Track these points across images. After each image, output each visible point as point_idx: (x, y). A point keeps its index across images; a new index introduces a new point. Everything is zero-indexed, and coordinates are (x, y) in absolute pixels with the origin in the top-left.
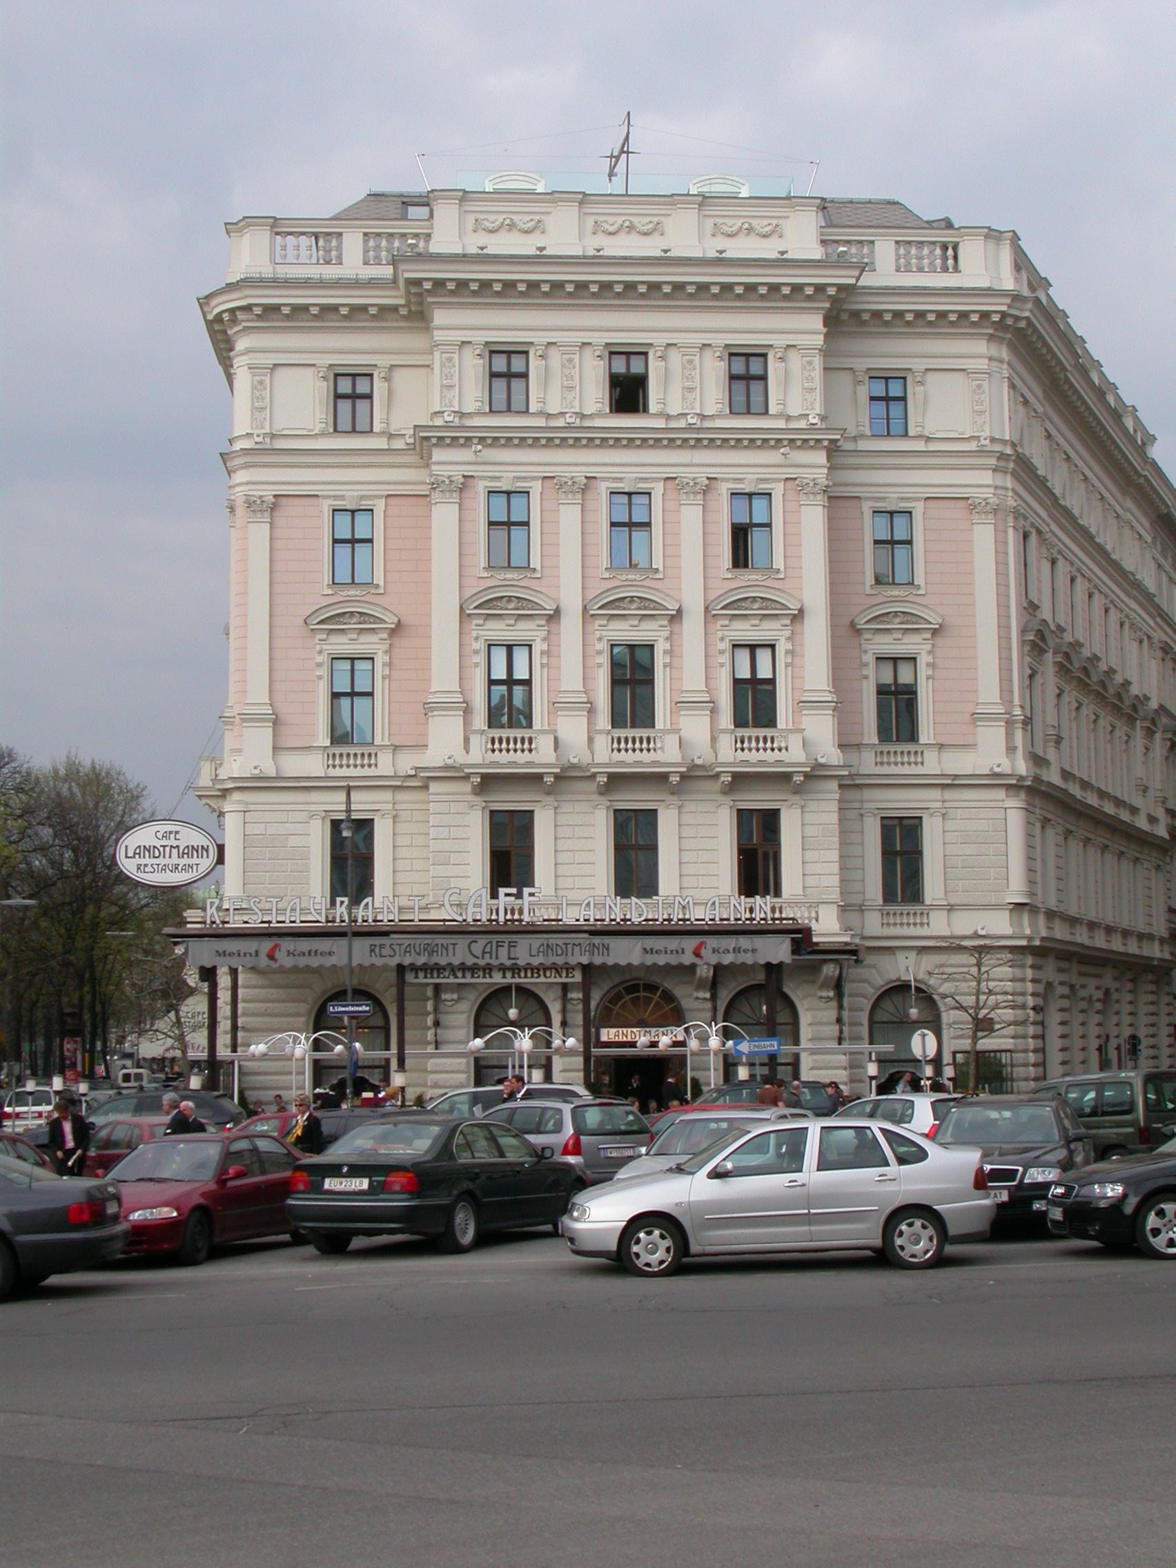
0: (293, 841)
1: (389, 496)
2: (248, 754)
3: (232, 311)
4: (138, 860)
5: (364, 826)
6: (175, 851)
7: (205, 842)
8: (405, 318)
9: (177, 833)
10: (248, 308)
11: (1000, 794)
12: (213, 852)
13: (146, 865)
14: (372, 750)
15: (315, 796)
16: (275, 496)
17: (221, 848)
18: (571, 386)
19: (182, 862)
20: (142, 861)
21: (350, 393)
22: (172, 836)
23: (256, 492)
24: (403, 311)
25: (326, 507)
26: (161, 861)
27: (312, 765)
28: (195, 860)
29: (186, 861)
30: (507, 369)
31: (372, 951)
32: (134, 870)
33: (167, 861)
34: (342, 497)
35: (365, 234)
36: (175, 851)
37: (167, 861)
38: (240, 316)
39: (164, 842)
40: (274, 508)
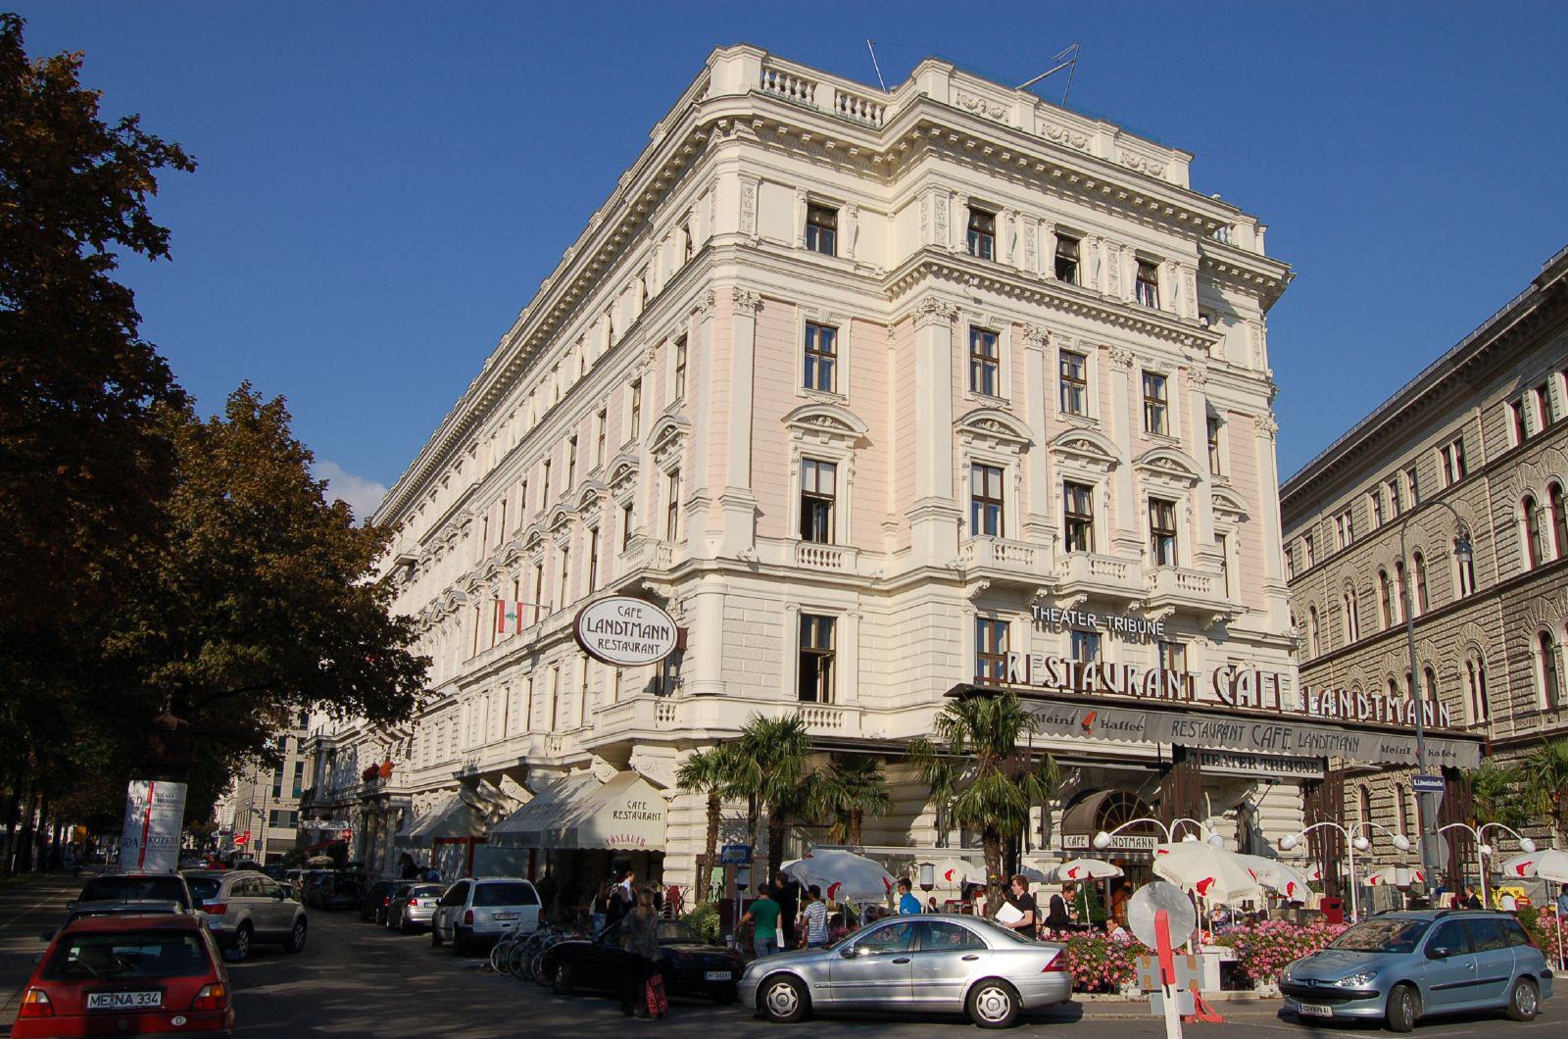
0: (766, 630)
1: (854, 319)
2: (715, 536)
3: (732, 120)
4: (599, 635)
5: (827, 623)
6: (636, 629)
7: (666, 625)
9: (639, 610)
10: (747, 120)
13: (607, 641)
14: (832, 550)
15: (786, 587)
16: (763, 297)
17: (682, 634)
19: (643, 641)
20: (604, 636)
21: (821, 222)
22: (635, 613)
23: (745, 287)
24: (877, 159)
26: (622, 638)
28: (655, 642)
29: (643, 641)
31: (1175, 728)
32: (596, 645)
35: (837, 91)
36: (636, 629)
38: (738, 125)
39: (627, 619)
40: (759, 307)
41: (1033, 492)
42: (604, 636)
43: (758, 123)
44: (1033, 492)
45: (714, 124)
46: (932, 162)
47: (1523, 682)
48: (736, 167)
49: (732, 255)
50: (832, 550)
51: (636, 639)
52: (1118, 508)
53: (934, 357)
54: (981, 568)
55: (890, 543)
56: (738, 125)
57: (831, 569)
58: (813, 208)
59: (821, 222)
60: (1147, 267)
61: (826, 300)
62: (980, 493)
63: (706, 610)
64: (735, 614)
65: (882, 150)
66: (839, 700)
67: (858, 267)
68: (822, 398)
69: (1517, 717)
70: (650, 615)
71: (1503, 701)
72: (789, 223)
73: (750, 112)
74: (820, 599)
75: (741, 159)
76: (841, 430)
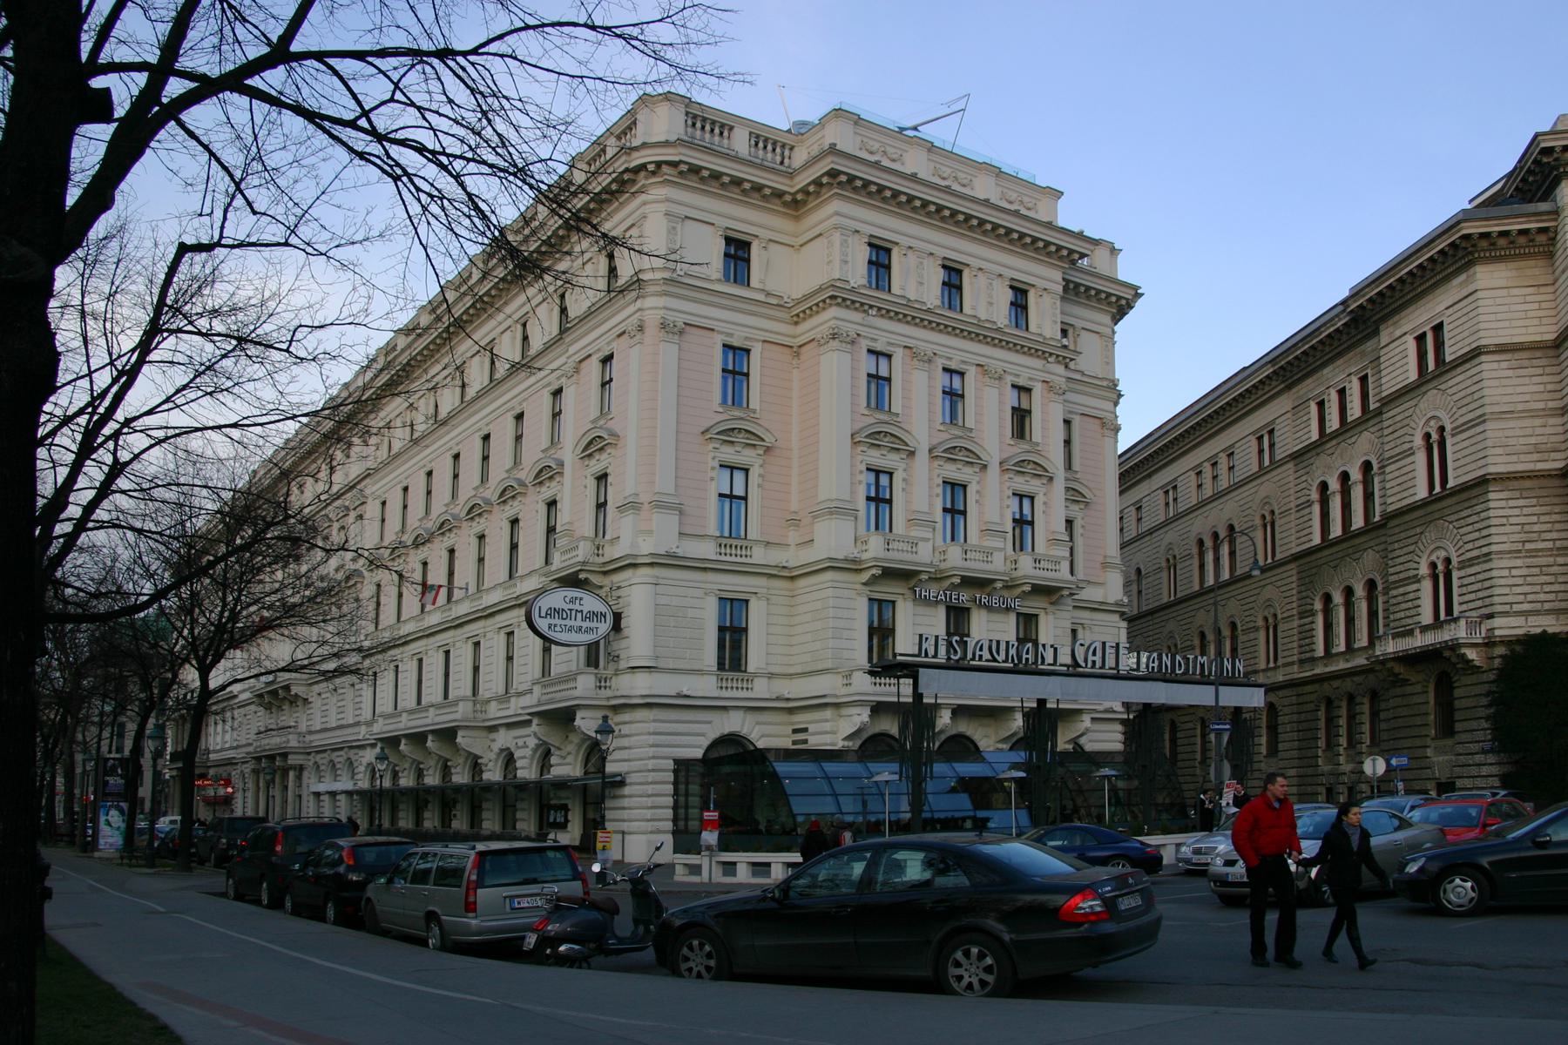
0: (691, 613)
3: (659, 164)
4: (549, 620)
8: (785, 204)
10: (674, 164)
11: (1116, 617)
12: (610, 618)
14: (745, 543)
15: (711, 576)
17: (617, 617)
18: (917, 280)
19: (585, 625)
20: (553, 621)
21: (738, 251)
23: (671, 317)
25: (719, 340)
26: (568, 622)
27: (707, 550)
29: (585, 625)
30: (880, 258)
33: (572, 623)
34: (731, 335)
37: (572, 623)
38: (665, 169)
41: (918, 492)
42: (553, 621)
43: (684, 168)
44: (918, 492)
45: (643, 167)
46: (836, 205)
47: (1306, 634)
48: (663, 207)
49: (658, 288)
50: (745, 543)
51: (579, 623)
52: (991, 503)
53: (836, 378)
54: (876, 559)
55: (793, 537)
56: (665, 169)
57: (743, 560)
58: (729, 241)
59: (738, 251)
60: (1020, 298)
61: (741, 326)
62: (873, 494)
63: (638, 597)
64: (663, 600)
65: (793, 190)
66: (751, 669)
67: (768, 294)
68: (737, 413)
69: (1301, 662)
70: (590, 603)
71: (1290, 649)
72: (709, 252)
73: (676, 159)
74: (736, 585)
75: (668, 200)
76: (753, 439)
